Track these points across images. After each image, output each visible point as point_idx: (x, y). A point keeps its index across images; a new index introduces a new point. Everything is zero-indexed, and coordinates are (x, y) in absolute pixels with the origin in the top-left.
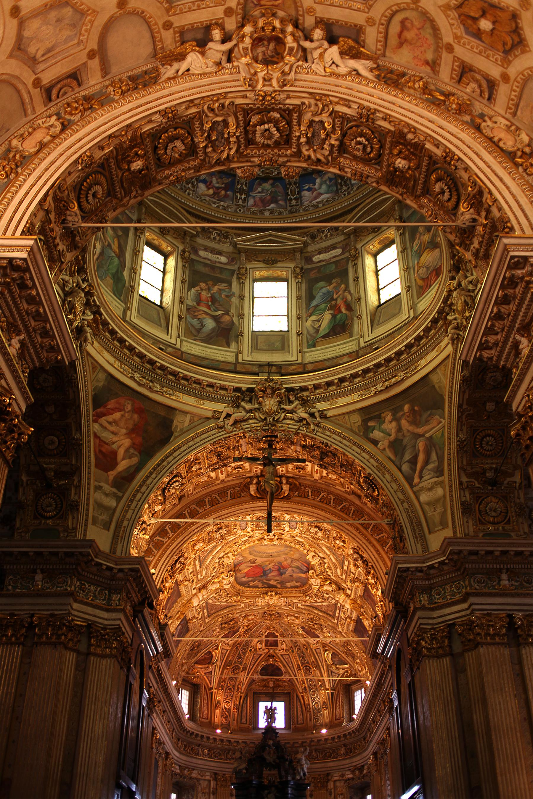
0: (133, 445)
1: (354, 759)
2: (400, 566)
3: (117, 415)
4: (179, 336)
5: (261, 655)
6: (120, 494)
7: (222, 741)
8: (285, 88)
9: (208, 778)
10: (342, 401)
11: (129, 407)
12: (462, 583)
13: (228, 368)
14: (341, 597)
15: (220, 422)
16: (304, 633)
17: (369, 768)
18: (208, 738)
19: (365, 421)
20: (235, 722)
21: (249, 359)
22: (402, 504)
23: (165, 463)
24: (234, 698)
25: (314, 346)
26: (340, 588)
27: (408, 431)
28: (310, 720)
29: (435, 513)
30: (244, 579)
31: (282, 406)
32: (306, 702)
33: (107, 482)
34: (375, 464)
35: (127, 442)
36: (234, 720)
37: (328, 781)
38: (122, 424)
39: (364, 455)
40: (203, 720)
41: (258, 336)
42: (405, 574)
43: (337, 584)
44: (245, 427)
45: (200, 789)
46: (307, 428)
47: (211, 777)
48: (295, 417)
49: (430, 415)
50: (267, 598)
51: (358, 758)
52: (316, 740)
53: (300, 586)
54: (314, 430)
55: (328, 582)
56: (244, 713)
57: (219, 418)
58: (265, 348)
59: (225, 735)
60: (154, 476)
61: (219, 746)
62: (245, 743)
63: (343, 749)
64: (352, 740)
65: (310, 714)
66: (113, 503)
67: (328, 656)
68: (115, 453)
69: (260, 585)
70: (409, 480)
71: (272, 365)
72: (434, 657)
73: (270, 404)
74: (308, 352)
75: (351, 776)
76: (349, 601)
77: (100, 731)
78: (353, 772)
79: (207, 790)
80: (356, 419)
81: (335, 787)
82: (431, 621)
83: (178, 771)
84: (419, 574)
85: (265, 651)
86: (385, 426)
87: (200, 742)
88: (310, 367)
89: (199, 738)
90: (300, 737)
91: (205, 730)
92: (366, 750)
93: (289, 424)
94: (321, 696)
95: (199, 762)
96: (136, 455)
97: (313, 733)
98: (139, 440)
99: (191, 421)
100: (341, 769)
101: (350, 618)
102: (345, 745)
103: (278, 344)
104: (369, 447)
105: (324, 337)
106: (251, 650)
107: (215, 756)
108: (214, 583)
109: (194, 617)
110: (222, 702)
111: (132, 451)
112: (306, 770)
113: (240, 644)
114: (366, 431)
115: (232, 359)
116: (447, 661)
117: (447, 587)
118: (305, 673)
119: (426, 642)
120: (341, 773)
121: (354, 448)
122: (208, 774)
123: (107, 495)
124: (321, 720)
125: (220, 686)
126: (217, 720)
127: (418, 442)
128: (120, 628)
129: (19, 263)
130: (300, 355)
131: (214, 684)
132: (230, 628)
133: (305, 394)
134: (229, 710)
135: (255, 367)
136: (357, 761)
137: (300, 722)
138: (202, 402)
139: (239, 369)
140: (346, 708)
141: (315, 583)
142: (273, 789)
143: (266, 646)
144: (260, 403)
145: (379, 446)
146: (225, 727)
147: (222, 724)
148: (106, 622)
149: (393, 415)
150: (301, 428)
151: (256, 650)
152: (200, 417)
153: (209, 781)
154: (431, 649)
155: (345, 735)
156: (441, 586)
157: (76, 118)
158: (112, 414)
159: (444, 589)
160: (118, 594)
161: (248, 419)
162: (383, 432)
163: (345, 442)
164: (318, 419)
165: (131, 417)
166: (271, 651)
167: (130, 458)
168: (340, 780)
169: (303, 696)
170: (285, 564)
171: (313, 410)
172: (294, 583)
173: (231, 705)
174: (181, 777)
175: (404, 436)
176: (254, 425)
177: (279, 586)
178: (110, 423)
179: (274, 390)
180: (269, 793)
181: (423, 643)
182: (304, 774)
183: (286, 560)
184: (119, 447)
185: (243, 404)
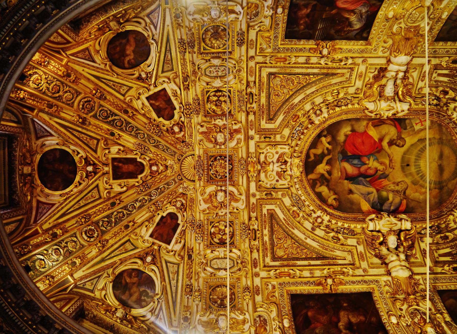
5: (95, 151)
16: (157, 219)
53: (330, 206)
69: (319, 151)
106: (112, 134)
143: (114, 159)
166: (106, 169)
169: (36, 233)
170: (385, 182)
173: (31, 87)
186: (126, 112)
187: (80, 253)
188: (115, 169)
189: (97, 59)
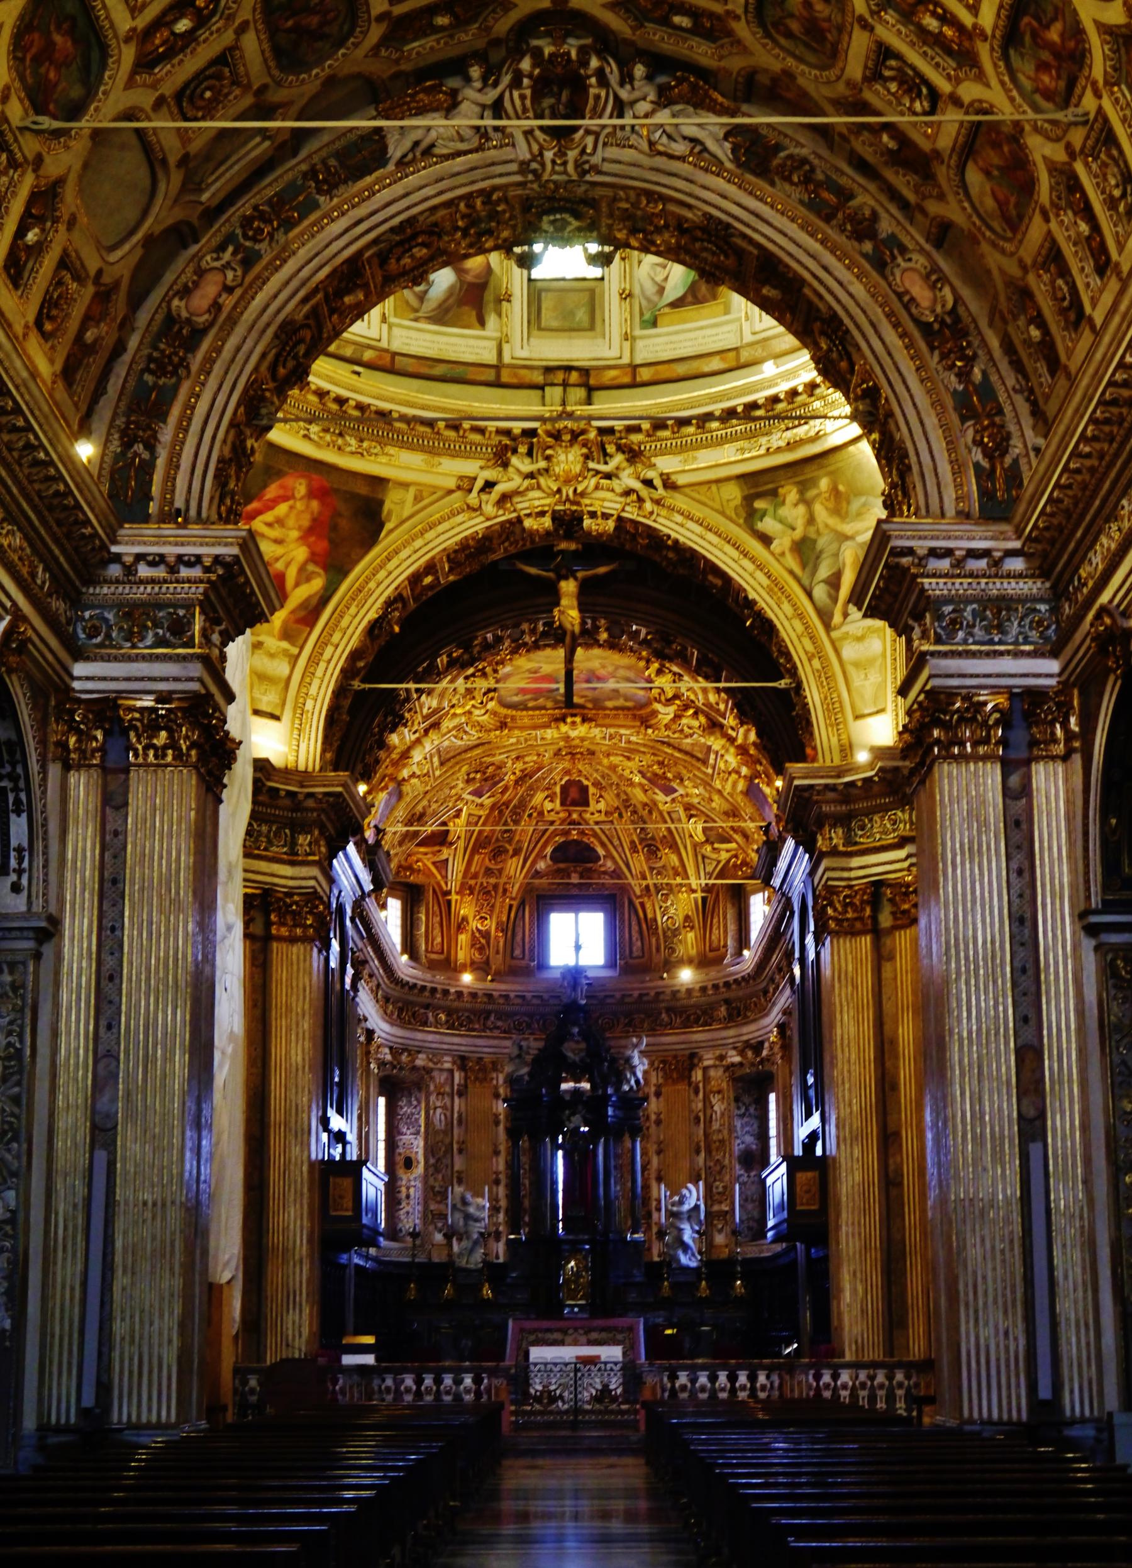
0: (313, 558)
1: (745, 1030)
2: (796, 782)
3: (282, 509)
4: (384, 319)
6: (295, 651)
7: (474, 995)
8: (588, 178)
9: (447, 1066)
10: (706, 458)
11: (301, 489)
12: (900, 814)
13: (483, 378)
14: (716, 743)
15: (473, 499)
16: (644, 781)
17: (771, 1049)
18: (446, 992)
19: (748, 500)
20: (500, 956)
21: (524, 354)
22: (810, 660)
23: (372, 585)
24: (497, 910)
25: (654, 324)
26: (714, 726)
27: (827, 526)
28: (658, 950)
29: (867, 683)
30: (516, 699)
31: (592, 465)
32: (650, 915)
33: (270, 633)
34: (765, 581)
35: (301, 553)
36: (497, 952)
37: (692, 1067)
38: (291, 522)
39: (746, 563)
40: (434, 956)
41: (540, 292)
42: (806, 794)
43: (707, 716)
44: (519, 506)
45: (432, 1088)
46: (640, 508)
47: (454, 1063)
48: (615, 484)
49: (864, 505)
50: (564, 728)
51: (752, 1027)
52: (668, 991)
54: (652, 513)
55: (691, 711)
56: (519, 938)
57: (470, 491)
58: (554, 324)
59: (480, 985)
60: (353, 610)
61: (468, 1006)
62: (523, 997)
63: (723, 1009)
64: (741, 993)
65: (658, 940)
66: (281, 668)
67: (696, 828)
68: (281, 578)
69: (549, 704)
70: (825, 617)
71: (569, 369)
72: (846, 934)
73: (568, 460)
74: (642, 338)
75: (737, 1059)
76: (732, 750)
77: (299, 1058)
78: (742, 1053)
79: (448, 1089)
80: (733, 494)
81: (706, 1079)
82: (846, 874)
83: (389, 1057)
84: (831, 795)
85: (562, 815)
86: (783, 511)
87: (429, 1001)
88: (645, 374)
89: (427, 994)
90: (636, 985)
91: (440, 978)
92: (767, 1015)
93: (603, 500)
94: (682, 905)
95: (430, 1037)
96: (319, 575)
97: (662, 978)
98: (322, 546)
99: (418, 499)
100: (719, 1048)
101: (738, 772)
102: (727, 1002)
103: (582, 315)
104: (755, 546)
105: (677, 304)
106: (530, 816)
107: (461, 1025)
108: (455, 715)
109: (413, 775)
110: (470, 919)
111: (311, 567)
112: (640, 1075)
113: (507, 804)
114: (750, 516)
115: (490, 358)
116: (866, 941)
117: (876, 818)
118: (648, 860)
119: (835, 910)
120: (718, 1053)
121: (728, 548)
122: (446, 1058)
123: (272, 656)
124: (681, 951)
125: (466, 888)
126: (462, 954)
127: (843, 548)
128: (316, 892)
129: (228, 559)
130: (627, 345)
131: (454, 884)
132: (486, 778)
133: (635, 438)
134: (486, 935)
135: (536, 373)
136: (749, 1032)
137: (635, 954)
138: (437, 459)
139: (505, 378)
140: (732, 927)
141: (666, 713)
142: (580, 1107)
143: (562, 804)
144: (548, 458)
145: (772, 547)
146: (481, 968)
147: (473, 963)
148: (291, 883)
149: (802, 492)
150: (628, 508)
151: (541, 814)
152: (434, 489)
153: (451, 1071)
154: (842, 920)
155: (727, 984)
156: (867, 815)
157: (262, 247)
158: (272, 508)
159: (871, 820)
160: (307, 833)
161: (527, 489)
162: (781, 522)
163: (710, 536)
164: (661, 491)
165: (307, 507)
167: (308, 580)
168: (715, 1066)
169: (642, 905)
171: (650, 474)
172: (620, 702)
173: (491, 924)
174: (394, 1067)
175: (818, 532)
176: (537, 503)
177: (590, 705)
178: (269, 525)
179: (575, 435)
180: (573, 1114)
181: (830, 911)
182: (637, 1082)
183: (604, 667)
184: (288, 565)
185: (515, 460)
186: (501, 813)
187: (671, 872)
188: (574, 803)
189: (444, 857)
